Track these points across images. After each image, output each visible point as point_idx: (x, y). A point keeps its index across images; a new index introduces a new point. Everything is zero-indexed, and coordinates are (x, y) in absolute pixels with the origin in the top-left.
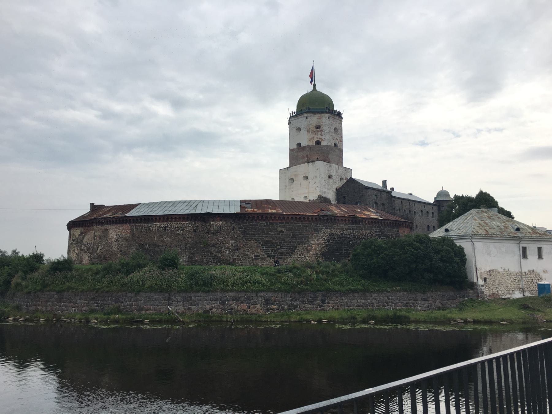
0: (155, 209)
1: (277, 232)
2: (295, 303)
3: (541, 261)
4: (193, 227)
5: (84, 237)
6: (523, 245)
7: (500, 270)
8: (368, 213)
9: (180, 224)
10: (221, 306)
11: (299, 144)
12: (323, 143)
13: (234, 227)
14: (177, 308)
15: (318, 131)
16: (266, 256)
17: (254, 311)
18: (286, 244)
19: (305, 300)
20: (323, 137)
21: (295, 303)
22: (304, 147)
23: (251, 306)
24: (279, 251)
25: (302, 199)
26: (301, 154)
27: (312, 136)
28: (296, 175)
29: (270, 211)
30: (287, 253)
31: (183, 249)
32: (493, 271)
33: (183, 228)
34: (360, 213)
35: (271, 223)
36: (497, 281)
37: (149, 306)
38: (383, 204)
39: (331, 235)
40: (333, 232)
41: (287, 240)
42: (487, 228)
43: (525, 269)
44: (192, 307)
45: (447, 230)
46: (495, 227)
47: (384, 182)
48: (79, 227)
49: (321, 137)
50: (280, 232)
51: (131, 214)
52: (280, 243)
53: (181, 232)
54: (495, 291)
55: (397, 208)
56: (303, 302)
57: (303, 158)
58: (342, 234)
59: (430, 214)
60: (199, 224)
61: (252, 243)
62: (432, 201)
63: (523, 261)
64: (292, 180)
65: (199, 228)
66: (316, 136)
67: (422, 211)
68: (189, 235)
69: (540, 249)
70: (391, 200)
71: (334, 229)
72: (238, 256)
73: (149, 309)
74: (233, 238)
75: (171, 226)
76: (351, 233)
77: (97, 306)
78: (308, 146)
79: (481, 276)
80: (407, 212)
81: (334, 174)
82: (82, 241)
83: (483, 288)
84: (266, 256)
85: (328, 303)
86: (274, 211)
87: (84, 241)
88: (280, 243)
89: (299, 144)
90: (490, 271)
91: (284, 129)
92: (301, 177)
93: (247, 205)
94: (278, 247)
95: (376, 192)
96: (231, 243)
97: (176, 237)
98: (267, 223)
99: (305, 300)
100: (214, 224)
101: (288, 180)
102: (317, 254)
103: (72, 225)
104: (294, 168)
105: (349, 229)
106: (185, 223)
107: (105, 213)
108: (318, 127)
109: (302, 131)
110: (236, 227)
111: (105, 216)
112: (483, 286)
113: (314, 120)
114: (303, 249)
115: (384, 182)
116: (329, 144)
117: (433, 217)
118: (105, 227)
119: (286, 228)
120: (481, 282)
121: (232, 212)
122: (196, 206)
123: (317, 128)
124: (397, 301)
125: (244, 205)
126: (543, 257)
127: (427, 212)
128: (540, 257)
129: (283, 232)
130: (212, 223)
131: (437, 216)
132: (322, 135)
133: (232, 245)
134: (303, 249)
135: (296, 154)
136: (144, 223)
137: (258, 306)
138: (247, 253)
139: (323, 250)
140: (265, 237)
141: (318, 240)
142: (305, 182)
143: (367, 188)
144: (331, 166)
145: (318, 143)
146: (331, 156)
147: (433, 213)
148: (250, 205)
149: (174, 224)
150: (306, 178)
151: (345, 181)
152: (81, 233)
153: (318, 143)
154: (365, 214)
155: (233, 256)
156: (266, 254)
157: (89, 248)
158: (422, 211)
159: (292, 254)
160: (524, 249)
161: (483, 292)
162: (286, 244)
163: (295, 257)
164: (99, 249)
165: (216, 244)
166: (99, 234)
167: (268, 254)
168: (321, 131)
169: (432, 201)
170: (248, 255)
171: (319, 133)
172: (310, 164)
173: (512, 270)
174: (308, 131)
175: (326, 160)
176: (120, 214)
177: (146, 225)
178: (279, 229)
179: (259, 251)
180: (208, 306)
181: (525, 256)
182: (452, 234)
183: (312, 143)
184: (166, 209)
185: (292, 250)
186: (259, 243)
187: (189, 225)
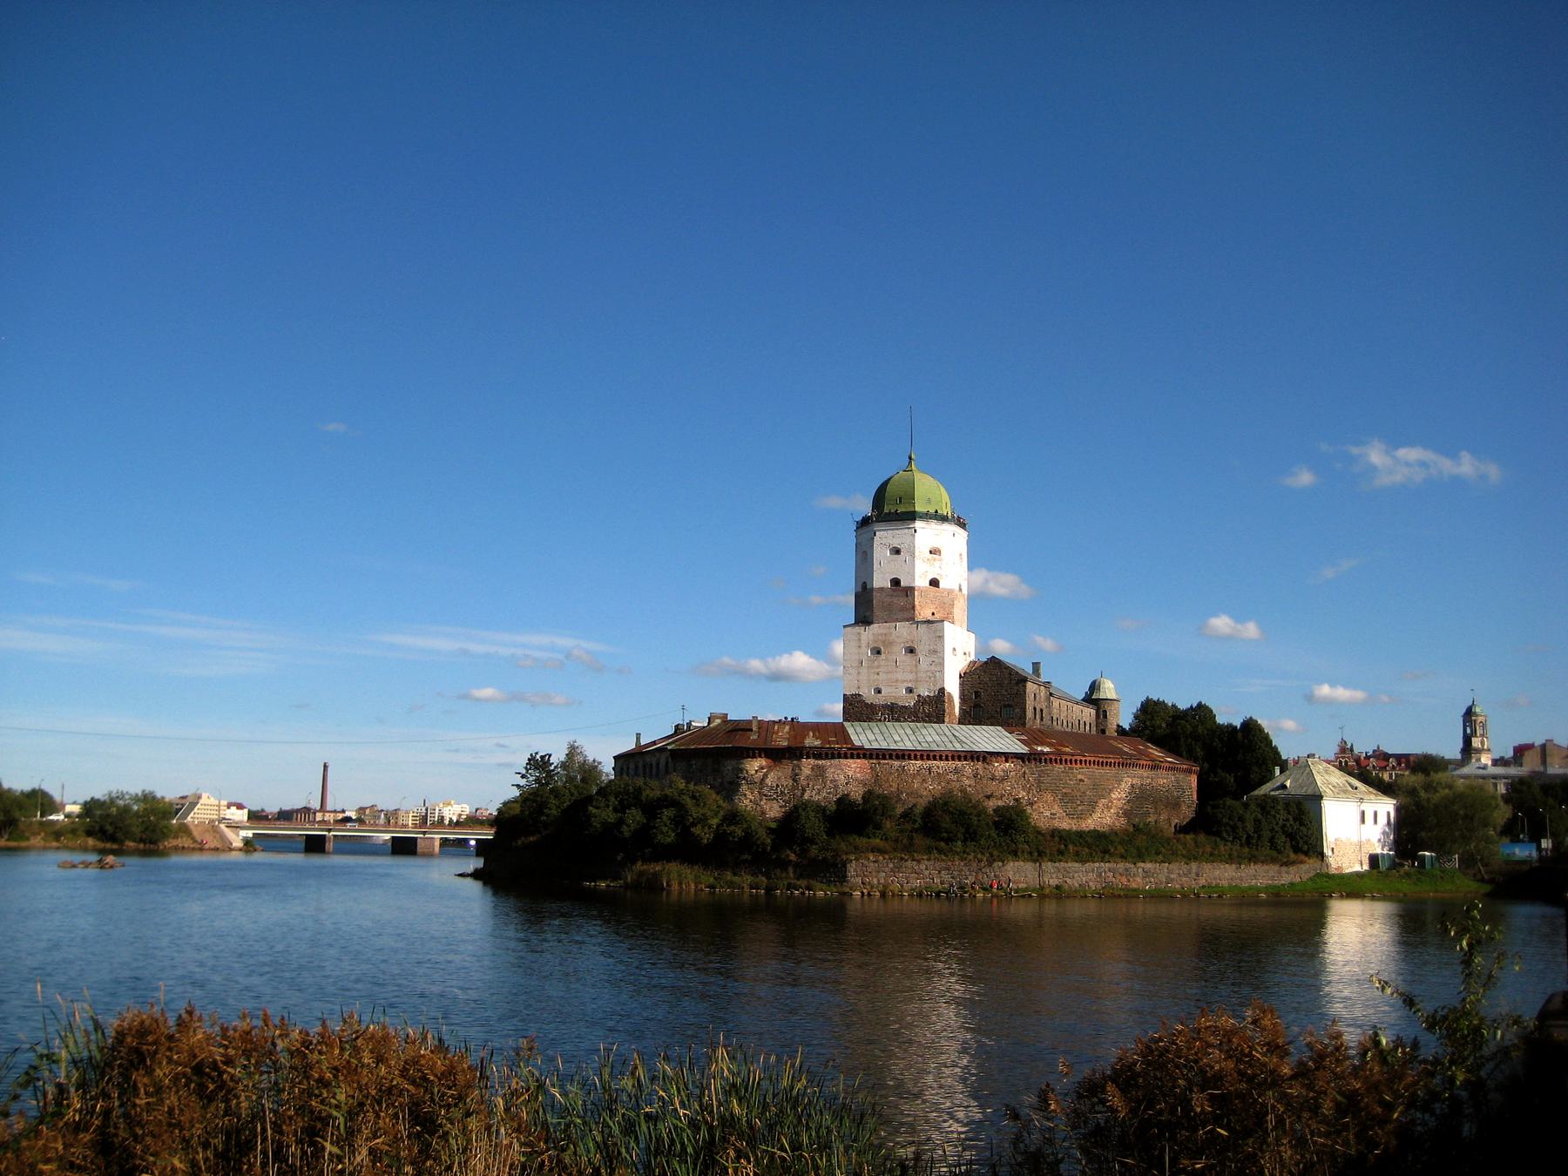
5: (765, 776)
6: (1364, 806)
17: (1134, 885)
26: (902, 602)
45: (1284, 787)
47: (1036, 666)
53: (954, 778)
60: (980, 765)
61: (1049, 797)
69: (1375, 814)
87: (768, 781)
89: (896, 582)
100: (999, 767)
115: (1036, 666)
135: (888, 599)
143: (1024, 680)
145: (934, 583)
149: (942, 764)
150: (911, 651)
153: (934, 583)
160: (1363, 813)
163: (1096, 816)
171: (937, 564)
177: (896, 763)
181: (1363, 821)
185: (1093, 805)
187: (968, 767)
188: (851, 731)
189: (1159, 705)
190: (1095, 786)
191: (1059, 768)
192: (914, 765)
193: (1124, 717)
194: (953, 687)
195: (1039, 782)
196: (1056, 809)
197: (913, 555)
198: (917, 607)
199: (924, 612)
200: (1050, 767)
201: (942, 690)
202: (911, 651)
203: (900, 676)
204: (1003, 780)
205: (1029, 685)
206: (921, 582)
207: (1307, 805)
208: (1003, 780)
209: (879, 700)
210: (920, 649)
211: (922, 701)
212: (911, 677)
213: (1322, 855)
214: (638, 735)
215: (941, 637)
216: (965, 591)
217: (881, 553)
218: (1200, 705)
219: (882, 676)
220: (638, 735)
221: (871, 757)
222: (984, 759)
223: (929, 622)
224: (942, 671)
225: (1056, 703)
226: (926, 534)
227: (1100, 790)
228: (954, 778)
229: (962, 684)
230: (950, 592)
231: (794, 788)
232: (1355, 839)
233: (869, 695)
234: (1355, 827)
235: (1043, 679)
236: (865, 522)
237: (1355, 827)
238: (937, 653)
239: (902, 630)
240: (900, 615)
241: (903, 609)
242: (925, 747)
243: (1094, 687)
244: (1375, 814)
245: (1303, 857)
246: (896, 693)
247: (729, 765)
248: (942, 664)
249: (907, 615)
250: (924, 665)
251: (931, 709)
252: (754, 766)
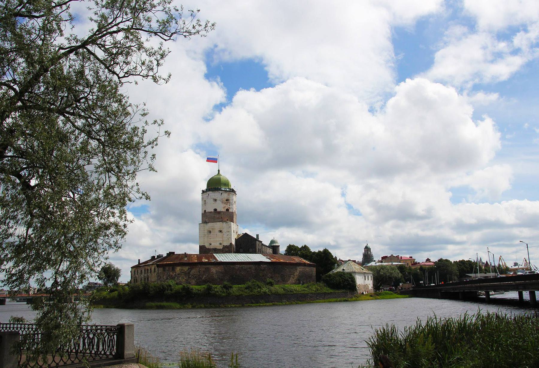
5: (190, 271)
9: (248, 266)
11: (215, 210)
12: (230, 210)
22: (219, 212)
26: (217, 216)
27: (225, 205)
28: (213, 229)
33: (250, 268)
45: (343, 270)
47: (257, 236)
53: (249, 270)
57: (218, 218)
78: (222, 212)
82: (189, 273)
89: (215, 210)
91: (198, 196)
92: (217, 231)
96: (269, 275)
101: (206, 231)
108: (227, 200)
109: (218, 201)
113: (225, 196)
115: (257, 236)
118: (207, 266)
145: (227, 210)
152: (189, 269)
153: (227, 210)
166: (203, 270)
169: (268, 245)
172: (224, 223)
174: (222, 202)
177: (232, 266)
183: (224, 210)
187: (253, 267)
188: (216, 256)
193: (282, 250)
194: (234, 243)
201: (231, 244)
202: (221, 231)
203: (218, 240)
204: (264, 270)
208: (264, 270)
209: (211, 247)
210: (224, 231)
211: (225, 247)
212: (221, 239)
214: (139, 260)
215: (230, 227)
218: (305, 246)
219: (212, 240)
220: (139, 260)
233: (207, 246)
234: (364, 282)
235: (260, 239)
236: (203, 192)
237: (364, 282)
238: (229, 232)
239: (218, 225)
242: (240, 261)
243: (272, 242)
246: (216, 244)
247: (178, 269)
250: (225, 236)
251: (227, 249)
252: (186, 269)
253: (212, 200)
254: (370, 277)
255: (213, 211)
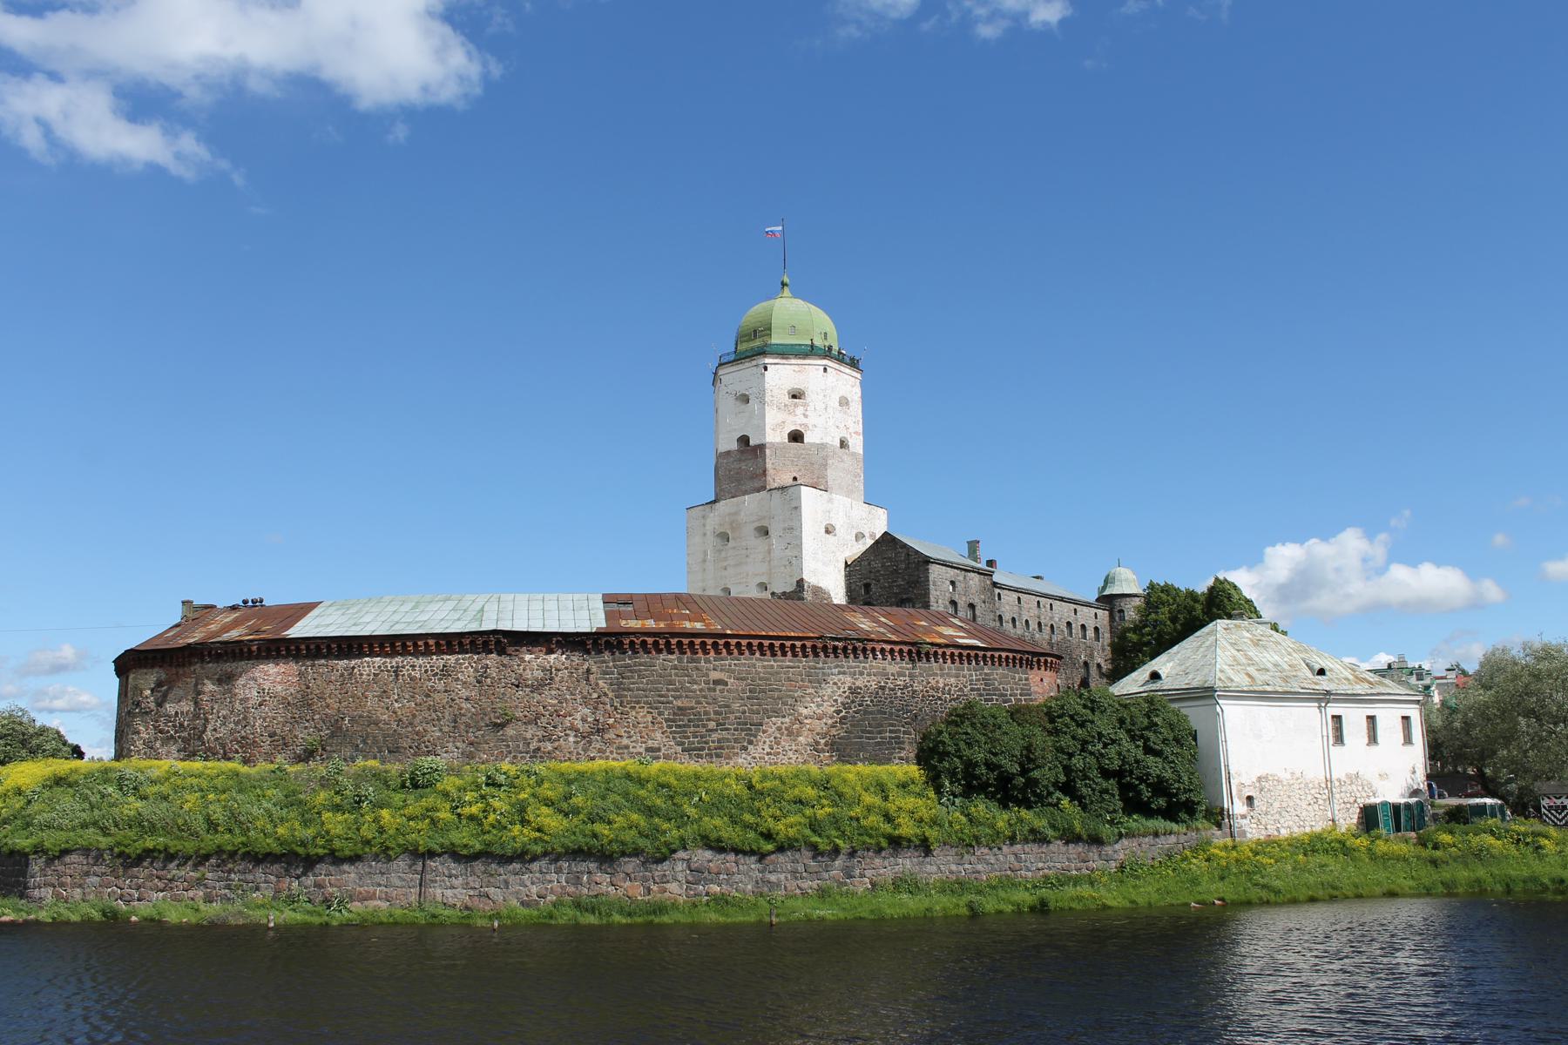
0: (367, 619)
1: (707, 683)
2: (773, 878)
3: (1374, 748)
4: (476, 670)
7: (1285, 776)
8: (949, 631)
9: (438, 661)
10: (571, 889)
13: (588, 670)
14: (449, 893)
15: (796, 405)
16: (679, 749)
18: (732, 717)
19: (801, 868)
20: (810, 421)
21: (773, 878)
23: (655, 888)
24: (715, 736)
25: (754, 593)
26: (748, 466)
28: (735, 525)
29: (688, 625)
30: (736, 741)
31: (446, 729)
32: (1266, 778)
33: (445, 672)
34: (927, 631)
35: (693, 661)
36: (1276, 805)
37: (371, 889)
38: (972, 606)
39: (854, 691)
40: (858, 683)
41: (736, 706)
42: (1251, 670)
43: (1338, 773)
44: (491, 890)
45: (1155, 676)
46: (1269, 666)
47: (973, 547)
48: (153, 667)
49: (805, 421)
50: (716, 682)
51: (298, 631)
52: (716, 713)
53: (440, 686)
54: (1272, 831)
55: (1007, 617)
56: (794, 872)
58: (883, 688)
59: (1090, 633)
60: (492, 659)
61: (642, 715)
62: (1092, 597)
63: (1338, 748)
64: (725, 537)
65: (493, 672)
66: (791, 418)
67: (1069, 624)
68: (464, 693)
69: (1371, 719)
70: (992, 593)
71: (861, 674)
72: (600, 751)
73: (372, 897)
74: (586, 701)
75: (413, 666)
76: (906, 687)
77: (228, 887)
79: (1240, 791)
80: (1033, 625)
81: (839, 522)
83: (1244, 822)
84: (679, 749)
85: (862, 876)
86: (699, 626)
88: (716, 713)
89: (744, 440)
90: (1260, 779)
92: (749, 530)
93: (622, 608)
94: (712, 725)
95: (952, 572)
96: (581, 715)
97: (428, 696)
98: (680, 660)
99: (801, 868)
100: (533, 662)
101: (711, 538)
102: (817, 743)
103: (127, 664)
104: (724, 506)
105: (901, 674)
106: (452, 659)
107: (227, 628)
110: (594, 669)
111: (225, 637)
112: (1244, 817)
114: (779, 729)
116: (827, 440)
117: (1097, 639)
118: (228, 667)
119: (733, 672)
120: (1239, 808)
121: (584, 627)
122: (482, 610)
123: (794, 397)
124: (1040, 865)
125: (615, 607)
126: (1379, 739)
127: (1083, 627)
128: (1373, 739)
129: (726, 684)
130: (528, 657)
131: (1107, 635)
132: (806, 416)
133: (584, 720)
134: (779, 729)
136: (339, 658)
137: (673, 887)
138: (625, 741)
139: (834, 732)
140: (675, 698)
141: (818, 706)
142: (759, 544)
143: (927, 561)
144: (830, 501)
145: (796, 437)
146: (831, 474)
147: (1096, 629)
148: (630, 608)
150: (765, 532)
151: (870, 542)
152: (159, 684)
153: (796, 437)
154: (941, 635)
155: (585, 750)
156: (678, 744)
157: (181, 725)
158: (1069, 624)
159: (751, 742)
161: (1244, 832)
162: (732, 717)
163: (760, 749)
164: (210, 727)
165: (538, 716)
167: (682, 744)
168: (805, 405)
170: (627, 747)
171: (800, 410)
173: (1309, 775)
175: (819, 485)
176: (268, 631)
178: (714, 675)
179: (658, 735)
180: (534, 889)
181: (1339, 739)
182: (1166, 683)
184: (396, 618)
185: (749, 730)
186: (660, 714)
187: (466, 665)
189: (1167, 589)
190: (755, 693)
191: (665, 661)
192: (370, 665)
195: (619, 688)
196: (658, 738)
197: (763, 403)
198: (770, 472)
199: (779, 474)
200: (644, 658)
204: (538, 687)
205: (935, 571)
206: (774, 434)
207: (1193, 714)
208: (538, 687)
213: (1217, 816)
215: (797, 508)
216: (857, 444)
217: (727, 404)
221: (297, 656)
222: (502, 652)
223: (783, 488)
224: (799, 557)
225: (1009, 598)
226: (779, 375)
227: (766, 703)
228: (440, 686)
229: (848, 576)
230: (822, 446)
231: (196, 716)
232: (1316, 773)
240: (750, 485)
241: (754, 477)
243: (1108, 581)
244: (1371, 719)
245: (1160, 824)
248: (799, 546)
249: (757, 485)
253: (731, 399)
254: (1389, 718)
255: (734, 446)
